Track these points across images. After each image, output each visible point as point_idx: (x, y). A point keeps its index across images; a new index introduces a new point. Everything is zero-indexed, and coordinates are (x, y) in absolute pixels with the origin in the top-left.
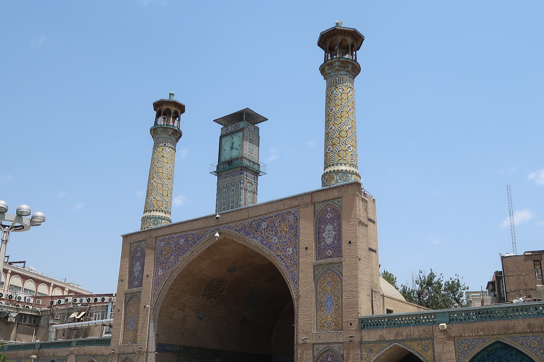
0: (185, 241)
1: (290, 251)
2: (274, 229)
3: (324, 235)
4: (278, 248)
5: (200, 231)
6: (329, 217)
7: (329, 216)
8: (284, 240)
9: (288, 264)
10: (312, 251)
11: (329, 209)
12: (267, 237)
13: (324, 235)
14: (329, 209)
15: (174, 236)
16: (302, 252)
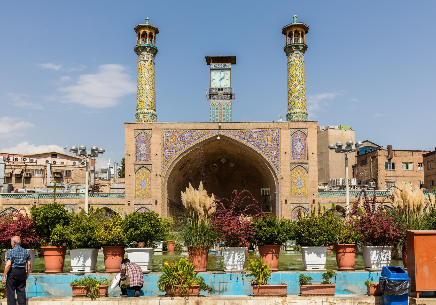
0: (190, 136)
1: (274, 153)
2: (262, 139)
3: (296, 147)
4: (266, 151)
5: (202, 131)
6: (299, 138)
7: (299, 137)
8: (270, 146)
9: (273, 160)
10: (289, 155)
11: (299, 133)
12: (258, 143)
13: (296, 147)
14: (299, 133)
15: (179, 131)
16: (283, 155)
